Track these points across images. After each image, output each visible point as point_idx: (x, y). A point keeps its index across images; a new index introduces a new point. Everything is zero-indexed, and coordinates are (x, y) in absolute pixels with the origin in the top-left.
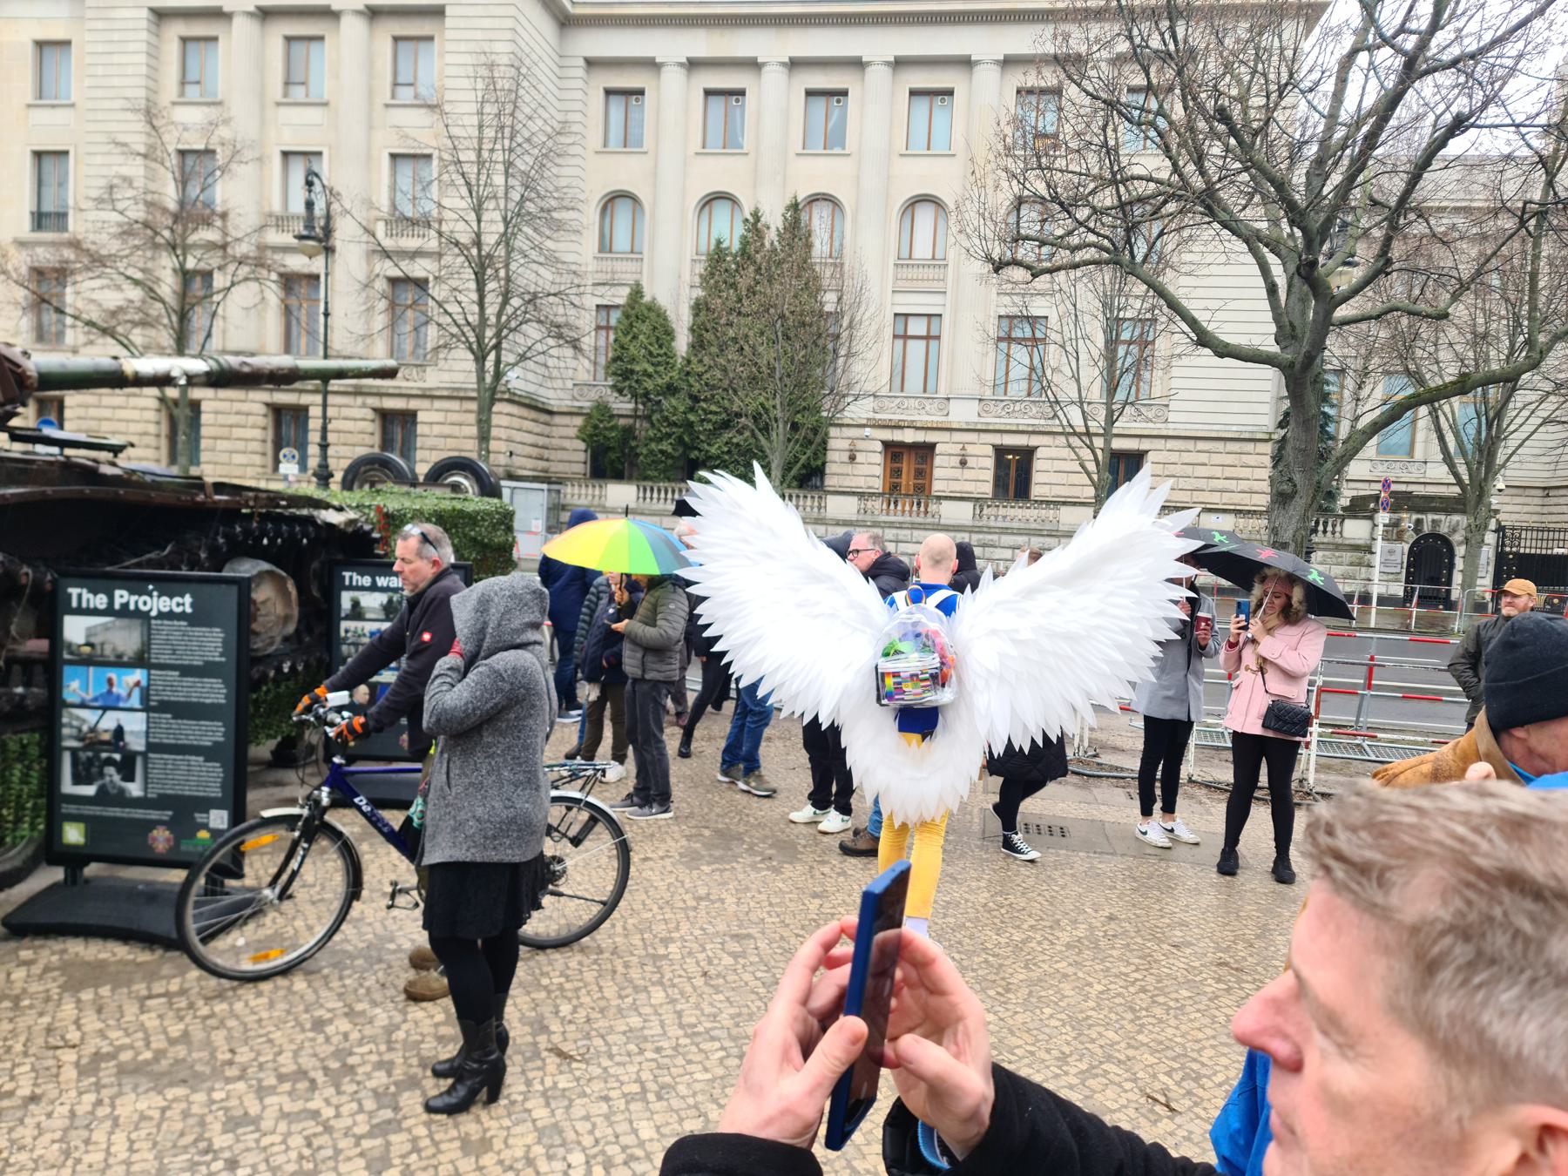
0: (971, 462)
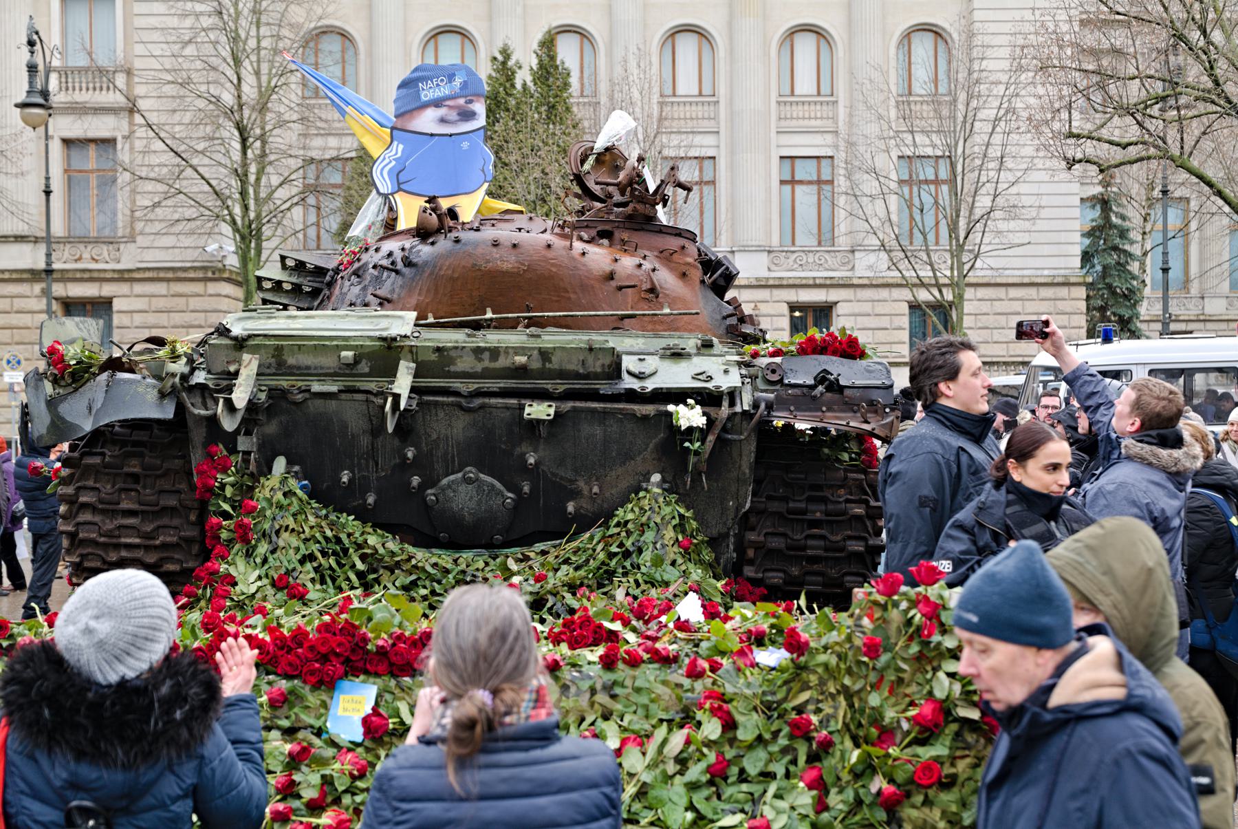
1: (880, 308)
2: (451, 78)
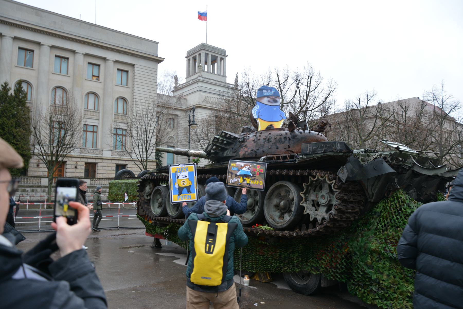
0: (78, 167)
1: (109, 165)
2: (271, 91)
